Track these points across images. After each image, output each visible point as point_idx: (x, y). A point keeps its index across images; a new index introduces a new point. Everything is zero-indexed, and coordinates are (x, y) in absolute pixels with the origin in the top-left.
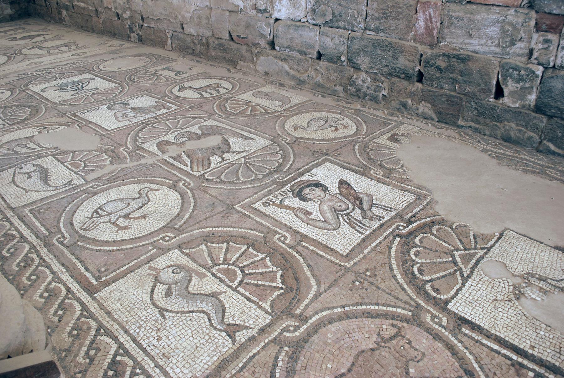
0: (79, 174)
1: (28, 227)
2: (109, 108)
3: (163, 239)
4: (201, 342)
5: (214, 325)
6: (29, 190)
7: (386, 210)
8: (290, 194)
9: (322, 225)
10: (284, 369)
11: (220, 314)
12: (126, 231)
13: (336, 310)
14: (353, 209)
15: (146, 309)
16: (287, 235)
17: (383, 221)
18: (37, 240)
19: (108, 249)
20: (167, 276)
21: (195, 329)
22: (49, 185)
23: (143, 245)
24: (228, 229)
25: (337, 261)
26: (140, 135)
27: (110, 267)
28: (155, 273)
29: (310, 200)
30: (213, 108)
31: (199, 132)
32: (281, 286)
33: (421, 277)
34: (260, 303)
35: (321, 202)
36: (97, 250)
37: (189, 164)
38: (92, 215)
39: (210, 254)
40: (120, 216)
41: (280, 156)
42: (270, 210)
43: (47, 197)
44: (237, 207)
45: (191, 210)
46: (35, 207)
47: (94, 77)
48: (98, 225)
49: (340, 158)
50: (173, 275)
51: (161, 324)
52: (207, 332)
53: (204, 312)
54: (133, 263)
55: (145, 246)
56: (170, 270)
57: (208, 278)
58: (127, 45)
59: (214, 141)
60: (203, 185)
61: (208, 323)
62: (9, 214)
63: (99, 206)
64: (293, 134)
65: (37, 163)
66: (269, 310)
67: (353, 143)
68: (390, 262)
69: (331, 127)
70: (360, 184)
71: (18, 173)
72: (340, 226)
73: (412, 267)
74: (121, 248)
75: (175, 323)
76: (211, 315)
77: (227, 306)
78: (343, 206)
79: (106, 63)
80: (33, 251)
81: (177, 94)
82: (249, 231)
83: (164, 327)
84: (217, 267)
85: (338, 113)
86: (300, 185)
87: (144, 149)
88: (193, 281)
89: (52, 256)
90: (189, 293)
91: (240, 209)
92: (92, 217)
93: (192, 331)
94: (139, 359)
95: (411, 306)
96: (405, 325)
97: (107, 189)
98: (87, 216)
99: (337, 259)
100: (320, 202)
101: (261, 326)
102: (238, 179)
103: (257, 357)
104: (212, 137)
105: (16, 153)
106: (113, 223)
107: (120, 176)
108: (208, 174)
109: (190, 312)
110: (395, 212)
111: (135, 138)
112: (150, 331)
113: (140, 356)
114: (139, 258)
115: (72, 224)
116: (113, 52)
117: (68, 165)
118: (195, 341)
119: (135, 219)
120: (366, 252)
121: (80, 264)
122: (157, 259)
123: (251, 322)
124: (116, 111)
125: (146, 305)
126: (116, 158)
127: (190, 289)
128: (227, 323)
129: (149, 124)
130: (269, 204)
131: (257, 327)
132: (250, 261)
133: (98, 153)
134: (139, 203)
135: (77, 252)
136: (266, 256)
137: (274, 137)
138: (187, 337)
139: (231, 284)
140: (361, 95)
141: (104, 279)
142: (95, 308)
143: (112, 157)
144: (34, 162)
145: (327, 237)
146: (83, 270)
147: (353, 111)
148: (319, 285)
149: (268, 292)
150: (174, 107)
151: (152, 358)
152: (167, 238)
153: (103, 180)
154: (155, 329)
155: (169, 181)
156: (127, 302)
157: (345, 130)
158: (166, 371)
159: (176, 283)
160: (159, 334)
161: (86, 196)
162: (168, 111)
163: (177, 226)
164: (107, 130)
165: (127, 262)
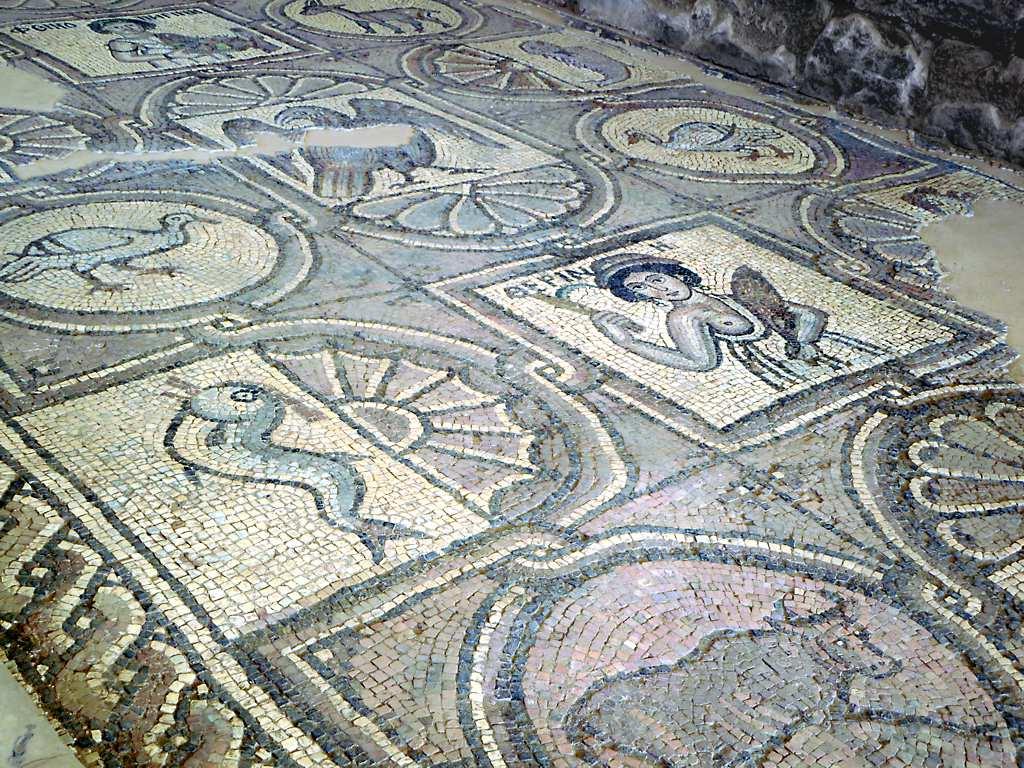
2: (96, 27)
3: (216, 324)
8: (591, 280)
9: (668, 357)
13: (669, 536)
14: (765, 335)
16: (563, 364)
17: (847, 371)
26: (178, 98)
28: (182, 393)
29: (643, 297)
31: (352, 113)
33: (928, 504)
37: (311, 179)
39: (341, 374)
40: (103, 261)
41: (576, 194)
44: (432, 288)
49: (750, 221)
50: (232, 402)
52: (311, 527)
54: (127, 365)
56: (228, 391)
57: (325, 423)
59: (394, 136)
60: (345, 228)
63: (47, 234)
64: (627, 152)
66: (487, 509)
67: (798, 193)
70: (792, 283)
72: (718, 364)
73: (909, 480)
74: (96, 328)
78: (738, 324)
81: (300, 18)
84: (356, 405)
92: (26, 253)
95: (884, 559)
96: (860, 597)
97: (73, 204)
100: (671, 307)
101: (457, 537)
106: (83, 272)
109: (269, 481)
110: (887, 357)
112: (156, 504)
113: (123, 549)
114: (145, 356)
118: (274, 541)
123: (431, 525)
129: (206, 78)
130: (525, 294)
132: (451, 405)
134: (161, 241)
137: (567, 150)
140: (846, 84)
141: (45, 388)
151: (154, 561)
152: (228, 324)
157: (779, 161)
158: (186, 589)
160: (177, 514)
162: (264, 54)
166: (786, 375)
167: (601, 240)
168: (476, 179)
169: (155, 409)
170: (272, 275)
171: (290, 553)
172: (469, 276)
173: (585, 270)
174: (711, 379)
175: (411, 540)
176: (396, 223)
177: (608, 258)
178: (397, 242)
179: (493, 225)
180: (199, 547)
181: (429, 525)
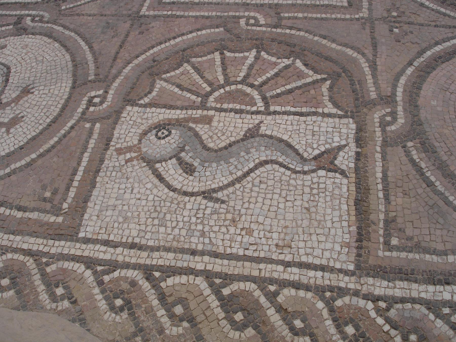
3: (90, 103)
5: (298, 169)
10: (432, 168)
11: (290, 151)
12: (22, 124)
15: (182, 206)
19: (23, 162)
20: (155, 146)
23: (72, 128)
24: (167, 44)
25: (348, 16)
28: (134, 155)
32: (319, 77)
34: (320, 110)
36: (9, 175)
45: (86, 48)
50: (163, 142)
51: (228, 212)
53: (266, 162)
55: (76, 128)
56: (152, 136)
61: (288, 173)
74: (41, 150)
75: (246, 200)
76: (281, 160)
77: (285, 137)
83: (237, 212)
84: (211, 98)
88: (201, 133)
90: (216, 151)
93: (280, 195)
94: (255, 273)
103: (389, 174)
118: (298, 203)
122: (116, 135)
125: (176, 202)
127: (211, 145)
128: (311, 157)
131: (349, 140)
139: (254, 109)
141: (65, 206)
142: (105, 252)
148: (363, 55)
149: (312, 92)
154: (227, 223)
155: (7, 28)
156: (142, 214)
159: (182, 149)
160: (240, 226)
163: (92, 77)
169: (134, 174)
175: (341, 154)
180: (275, 236)
181: (336, 139)
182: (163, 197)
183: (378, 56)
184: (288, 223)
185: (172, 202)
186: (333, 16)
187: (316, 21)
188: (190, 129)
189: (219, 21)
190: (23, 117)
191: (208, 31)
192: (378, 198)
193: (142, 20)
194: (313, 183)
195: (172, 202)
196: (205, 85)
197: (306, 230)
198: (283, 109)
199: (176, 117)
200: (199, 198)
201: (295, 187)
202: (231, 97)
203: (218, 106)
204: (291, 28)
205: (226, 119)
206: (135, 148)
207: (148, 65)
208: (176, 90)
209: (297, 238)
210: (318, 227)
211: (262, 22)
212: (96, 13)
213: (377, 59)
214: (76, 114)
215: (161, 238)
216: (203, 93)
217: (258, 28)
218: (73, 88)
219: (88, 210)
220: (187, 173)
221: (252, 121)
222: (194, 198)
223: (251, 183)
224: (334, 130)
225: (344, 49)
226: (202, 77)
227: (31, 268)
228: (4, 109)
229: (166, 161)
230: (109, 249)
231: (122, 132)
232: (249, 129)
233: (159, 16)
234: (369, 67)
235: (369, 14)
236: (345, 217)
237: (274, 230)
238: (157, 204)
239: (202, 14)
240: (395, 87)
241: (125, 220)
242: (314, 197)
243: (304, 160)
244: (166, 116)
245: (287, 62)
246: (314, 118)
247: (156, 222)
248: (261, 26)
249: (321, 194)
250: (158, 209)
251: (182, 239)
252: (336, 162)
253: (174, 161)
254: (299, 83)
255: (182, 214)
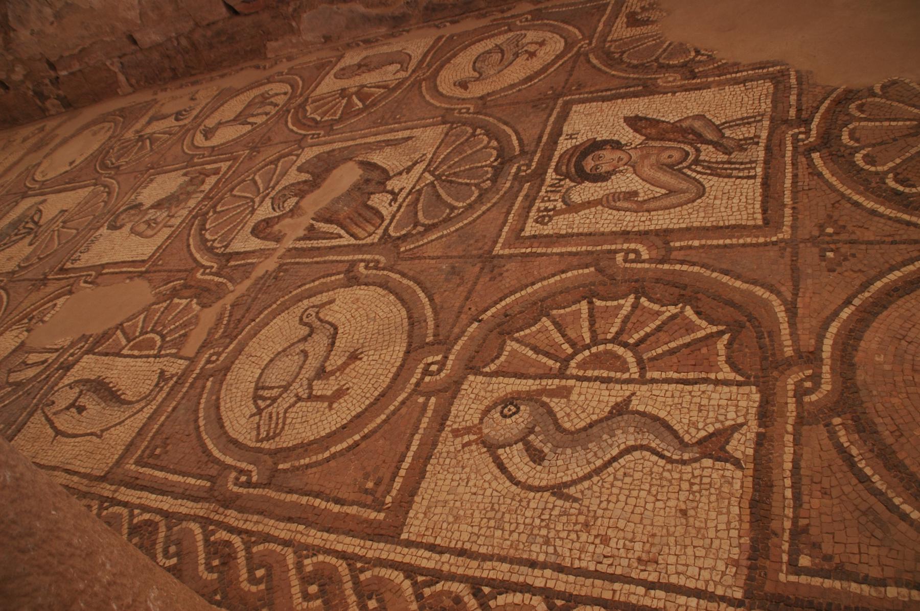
0: (167, 355)
1: (163, 493)
2: (113, 227)
3: (426, 372)
4: (682, 498)
5: (675, 457)
6: (102, 431)
7: (749, 123)
9: (673, 200)
10: (868, 455)
11: (667, 434)
12: (347, 397)
14: (698, 150)
15: (524, 503)
18: (199, 505)
21: (651, 485)
22: (130, 403)
23: (403, 403)
24: (523, 293)
25: (761, 240)
26: (208, 236)
27: (380, 474)
30: (292, 131)
31: (305, 176)
32: (714, 329)
34: (712, 376)
35: (633, 167)
36: (328, 460)
37: (342, 232)
38: (257, 407)
39: (536, 350)
42: (560, 224)
43: (145, 425)
44: (498, 250)
45: (425, 300)
46: (139, 452)
47: (41, 198)
48: (285, 418)
50: (509, 421)
51: (580, 513)
52: (677, 476)
53: (634, 448)
55: (408, 403)
58: (50, 124)
59: (347, 176)
61: (662, 462)
62: (106, 490)
63: (253, 385)
65: (72, 379)
68: (843, 195)
69: (516, 55)
71: (54, 414)
74: (366, 431)
75: (604, 498)
76: (653, 445)
77: (662, 414)
78: (677, 155)
79: (41, 169)
80: (211, 528)
82: (564, 276)
83: (592, 514)
84: (573, 363)
85: (506, 32)
86: (569, 161)
87: (238, 253)
88: (556, 409)
89: (255, 518)
90: (572, 433)
91: (507, 251)
92: (260, 411)
93: (649, 492)
94: (607, 595)
97: (239, 351)
98: (248, 413)
99: (758, 237)
100: (631, 169)
102: (453, 208)
103: (803, 464)
104: (336, 173)
105: (19, 385)
107: (239, 317)
108: (391, 229)
111: (205, 245)
114: (418, 428)
115: (235, 442)
116: (37, 147)
117: (130, 352)
118: (672, 503)
119: (342, 368)
120: (787, 200)
121: (318, 501)
124: (129, 226)
125: (518, 498)
126: (205, 294)
127: (567, 425)
128: (694, 440)
129: (207, 213)
131: (749, 417)
133: (165, 305)
135: (294, 483)
136: (637, 298)
138: (649, 506)
139: (626, 376)
141: (389, 499)
142: (428, 559)
143: (197, 296)
144: (66, 381)
145: (702, 214)
146: (336, 508)
147: (529, 17)
148: (779, 294)
149: (704, 350)
150: (224, 166)
153: (216, 340)
154: (578, 527)
156: (476, 514)
159: (531, 431)
160: (594, 532)
161: (214, 382)
162: (218, 177)
163: (430, 339)
164: (143, 261)
165: (402, 448)
166: (743, 166)
167: (538, 155)
168: (424, 167)
169: (471, 462)
170: (408, 311)
171: (689, 504)
172: (506, 229)
173: (556, 179)
174: (712, 197)
175: (736, 435)
176: (423, 225)
177: (558, 163)
178: (442, 237)
179: (473, 188)
181: (732, 415)
182: (504, 493)
183: (800, 294)
184: (656, 531)
185: (513, 499)
186: (741, 241)
187: (716, 251)
188: (544, 404)
189: (589, 259)
190: (348, 389)
191: (575, 272)
192: (784, 498)
193: (495, 262)
194: (694, 477)
195: (513, 499)
196: (566, 346)
197: (680, 540)
198: (664, 375)
199: (528, 389)
200: (547, 494)
201: (670, 481)
202: (597, 361)
203: (581, 373)
204: (682, 262)
205: (589, 390)
206: (475, 429)
207: (497, 321)
208: (530, 353)
209: (667, 551)
210: (697, 537)
211: (645, 256)
212: (440, 254)
213: (799, 300)
214: (408, 386)
215: (495, 544)
216: (563, 356)
217: (639, 266)
218: (408, 352)
219: (414, 506)
220: (534, 462)
221: (621, 393)
222: (540, 494)
223: (612, 476)
224: (729, 402)
225: (752, 287)
226: (564, 336)
227: (343, 574)
228: (328, 379)
229: (510, 445)
230: (434, 555)
231: (461, 408)
232: (617, 404)
233: (516, 255)
234: (787, 311)
235: (792, 234)
236: (735, 524)
237: (637, 539)
238: (495, 500)
239: (569, 249)
240: (820, 338)
241: (455, 520)
242: (694, 495)
243: (684, 445)
244: (515, 388)
245: (673, 310)
246: (703, 387)
247: (492, 523)
248: (644, 261)
249: (703, 491)
250: (496, 507)
251: (521, 546)
252: (728, 448)
253: (520, 445)
254: (687, 339)
255: (524, 515)
